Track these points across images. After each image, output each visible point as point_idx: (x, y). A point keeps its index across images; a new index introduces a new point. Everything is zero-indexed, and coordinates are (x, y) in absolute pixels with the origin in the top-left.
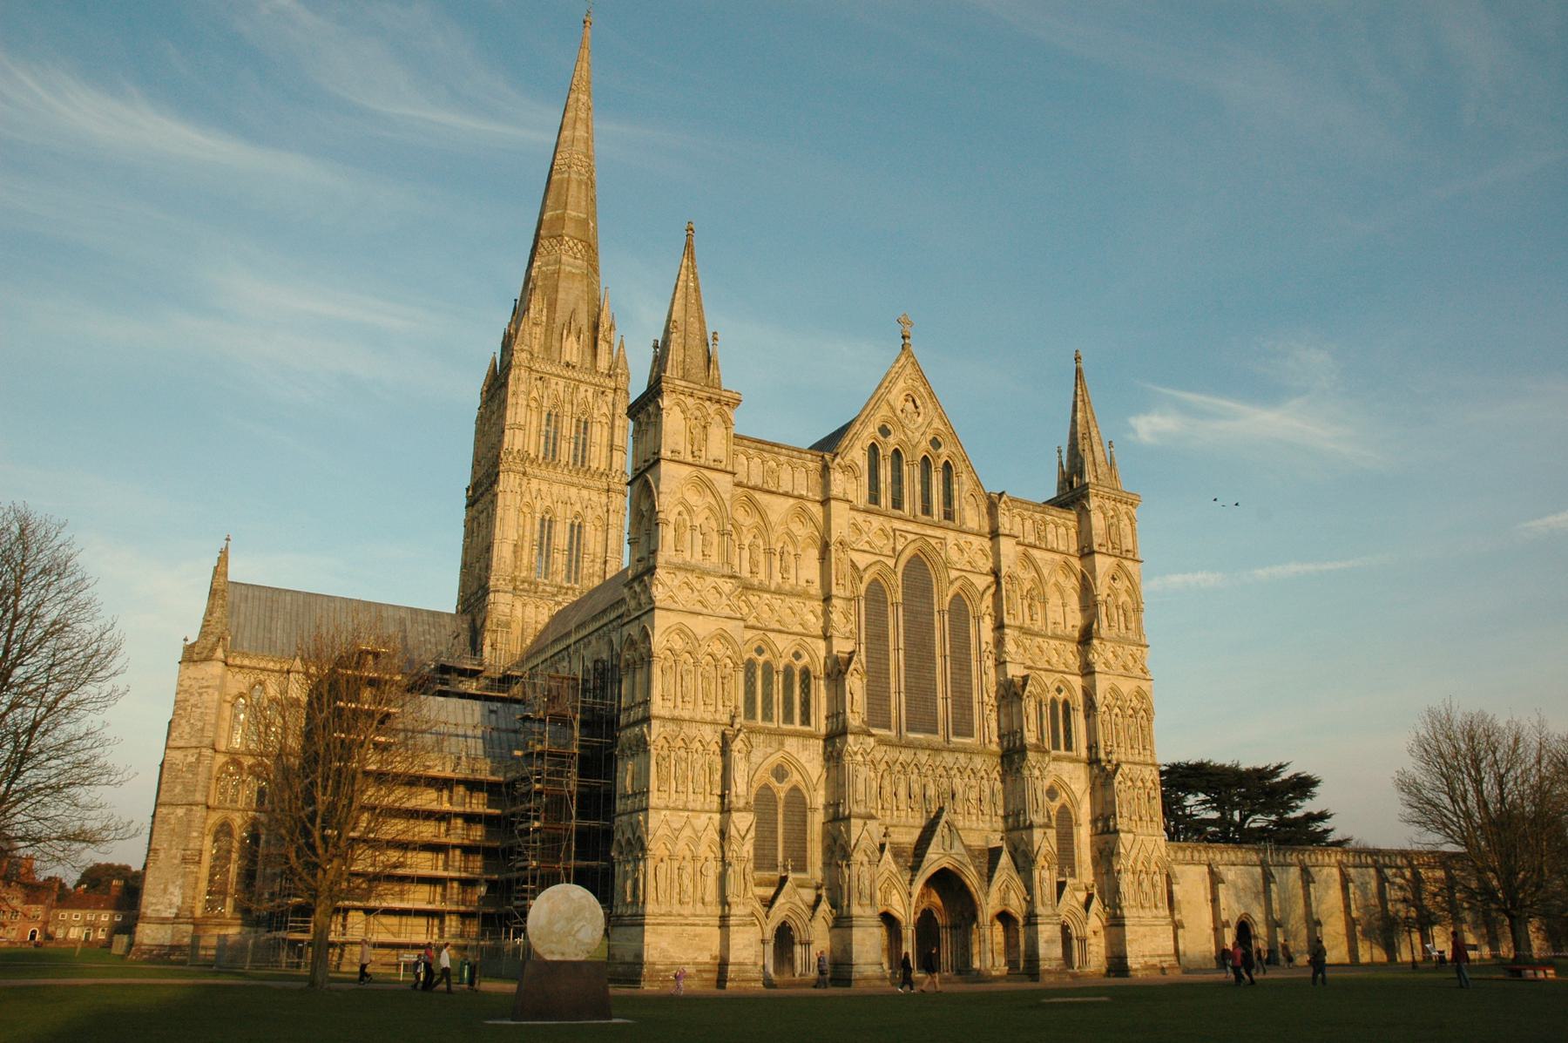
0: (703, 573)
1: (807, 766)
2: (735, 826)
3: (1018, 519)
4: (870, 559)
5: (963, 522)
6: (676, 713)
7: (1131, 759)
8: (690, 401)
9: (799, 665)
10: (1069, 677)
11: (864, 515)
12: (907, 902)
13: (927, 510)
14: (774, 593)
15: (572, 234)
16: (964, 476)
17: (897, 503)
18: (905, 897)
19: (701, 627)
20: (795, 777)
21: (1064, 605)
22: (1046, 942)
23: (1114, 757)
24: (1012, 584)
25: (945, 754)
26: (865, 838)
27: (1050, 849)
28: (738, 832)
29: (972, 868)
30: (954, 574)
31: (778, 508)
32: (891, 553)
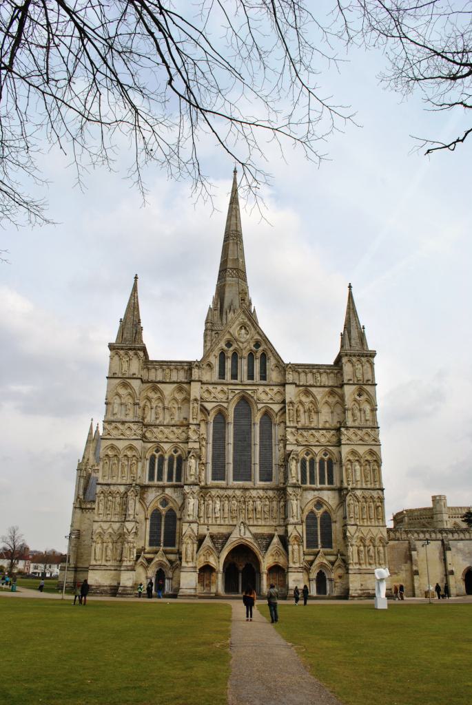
1: (176, 500)
3: (303, 374)
5: (271, 380)
7: (364, 486)
8: (122, 352)
9: (176, 455)
10: (330, 448)
13: (251, 377)
15: (231, 267)
16: (272, 358)
17: (234, 376)
18: (216, 557)
20: (171, 505)
21: (332, 412)
22: (294, 581)
23: (350, 487)
25: (251, 491)
28: (127, 530)
29: (255, 544)
30: (260, 406)
31: (168, 390)
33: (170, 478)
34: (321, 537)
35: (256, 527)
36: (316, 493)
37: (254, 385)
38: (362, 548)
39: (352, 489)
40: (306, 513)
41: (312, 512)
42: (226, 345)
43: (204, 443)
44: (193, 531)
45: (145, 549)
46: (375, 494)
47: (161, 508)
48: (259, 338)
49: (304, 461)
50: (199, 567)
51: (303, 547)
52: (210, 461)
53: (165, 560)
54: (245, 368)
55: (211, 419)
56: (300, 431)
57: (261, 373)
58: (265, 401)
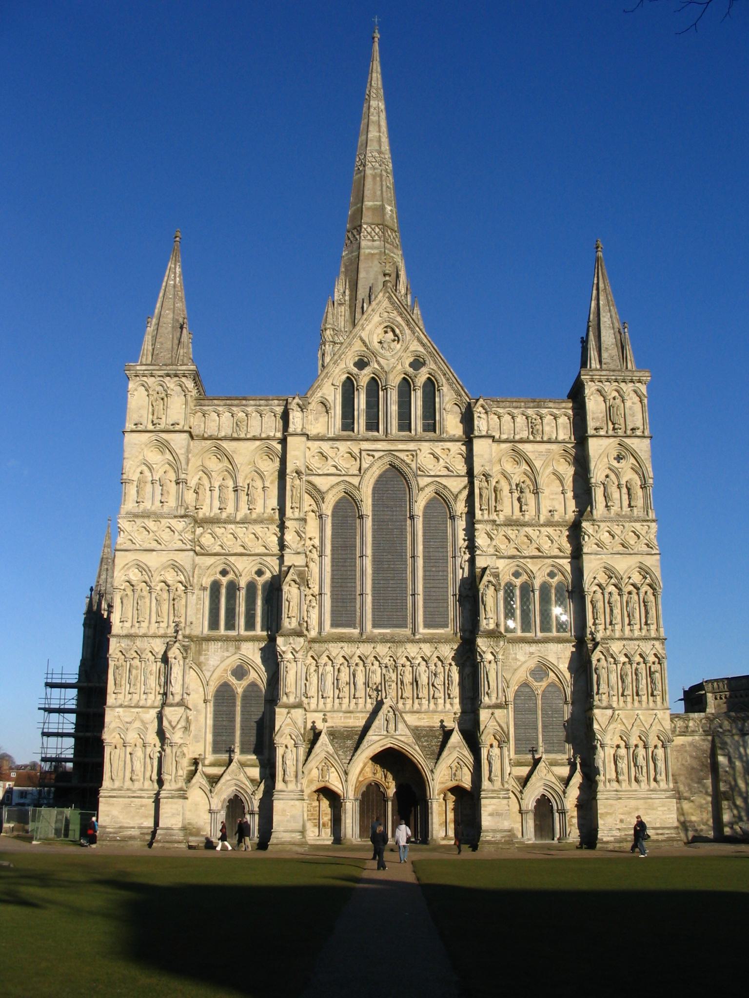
0: (157, 517)
2: (167, 719)
3: (507, 418)
4: (334, 480)
6: (133, 631)
8: (151, 381)
11: (330, 443)
12: (343, 778)
14: (238, 523)
15: (370, 221)
16: (445, 389)
17: (372, 425)
19: (152, 560)
22: (491, 815)
23: (599, 636)
24: (487, 481)
25: (409, 646)
26: (288, 725)
27: (498, 728)
28: (170, 723)
29: (417, 748)
32: (357, 472)
33: (250, 624)
34: (543, 732)
35: (418, 714)
36: (533, 648)
37: (412, 440)
38: (623, 751)
39: (602, 639)
40: (514, 687)
41: (525, 685)
42: (356, 365)
43: (315, 555)
44: (295, 723)
45: (205, 758)
46: (647, 648)
47: (233, 681)
48: (421, 349)
49: (509, 590)
50: (307, 792)
51: (509, 750)
52: (327, 590)
53: (242, 777)
54: (394, 408)
55: (328, 508)
56: (503, 530)
57: (425, 417)
58: (432, 473)
